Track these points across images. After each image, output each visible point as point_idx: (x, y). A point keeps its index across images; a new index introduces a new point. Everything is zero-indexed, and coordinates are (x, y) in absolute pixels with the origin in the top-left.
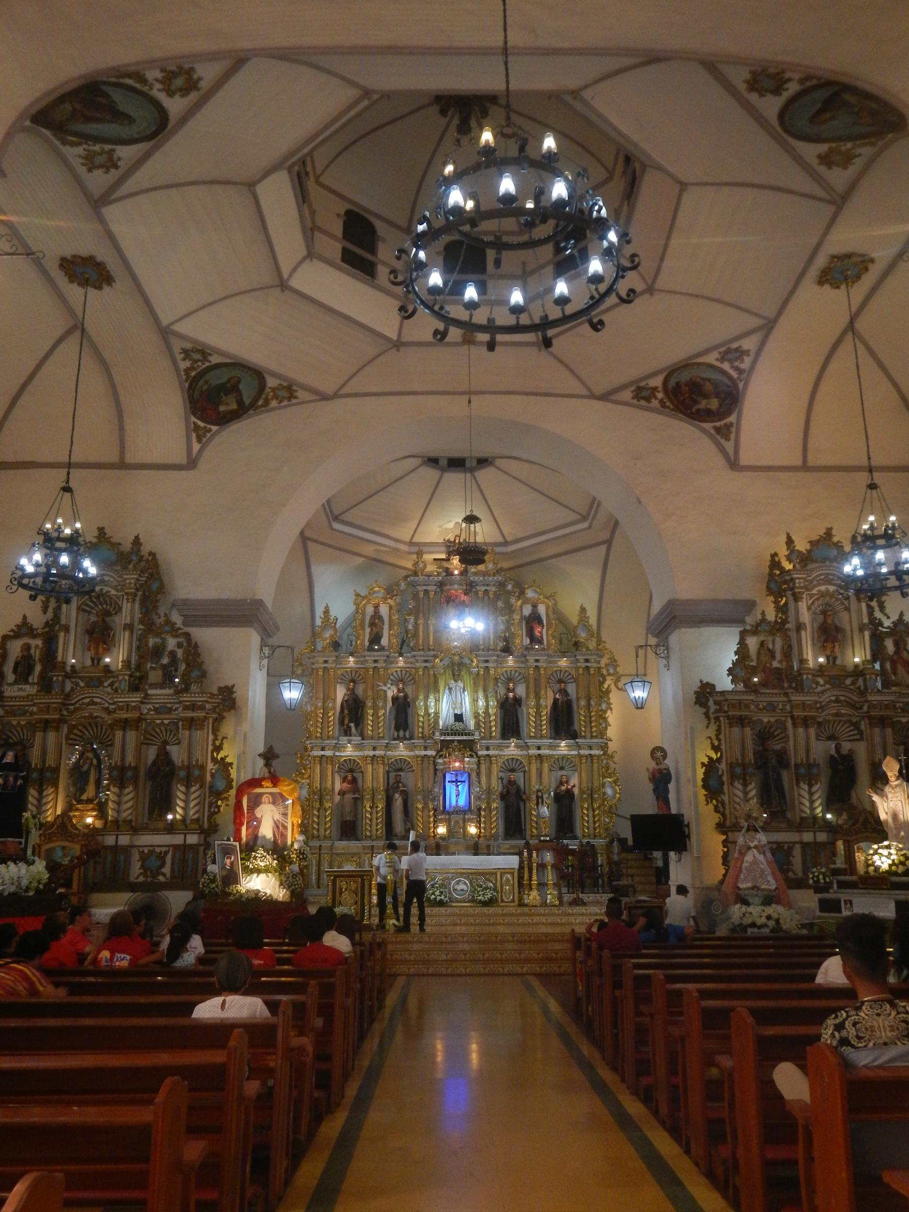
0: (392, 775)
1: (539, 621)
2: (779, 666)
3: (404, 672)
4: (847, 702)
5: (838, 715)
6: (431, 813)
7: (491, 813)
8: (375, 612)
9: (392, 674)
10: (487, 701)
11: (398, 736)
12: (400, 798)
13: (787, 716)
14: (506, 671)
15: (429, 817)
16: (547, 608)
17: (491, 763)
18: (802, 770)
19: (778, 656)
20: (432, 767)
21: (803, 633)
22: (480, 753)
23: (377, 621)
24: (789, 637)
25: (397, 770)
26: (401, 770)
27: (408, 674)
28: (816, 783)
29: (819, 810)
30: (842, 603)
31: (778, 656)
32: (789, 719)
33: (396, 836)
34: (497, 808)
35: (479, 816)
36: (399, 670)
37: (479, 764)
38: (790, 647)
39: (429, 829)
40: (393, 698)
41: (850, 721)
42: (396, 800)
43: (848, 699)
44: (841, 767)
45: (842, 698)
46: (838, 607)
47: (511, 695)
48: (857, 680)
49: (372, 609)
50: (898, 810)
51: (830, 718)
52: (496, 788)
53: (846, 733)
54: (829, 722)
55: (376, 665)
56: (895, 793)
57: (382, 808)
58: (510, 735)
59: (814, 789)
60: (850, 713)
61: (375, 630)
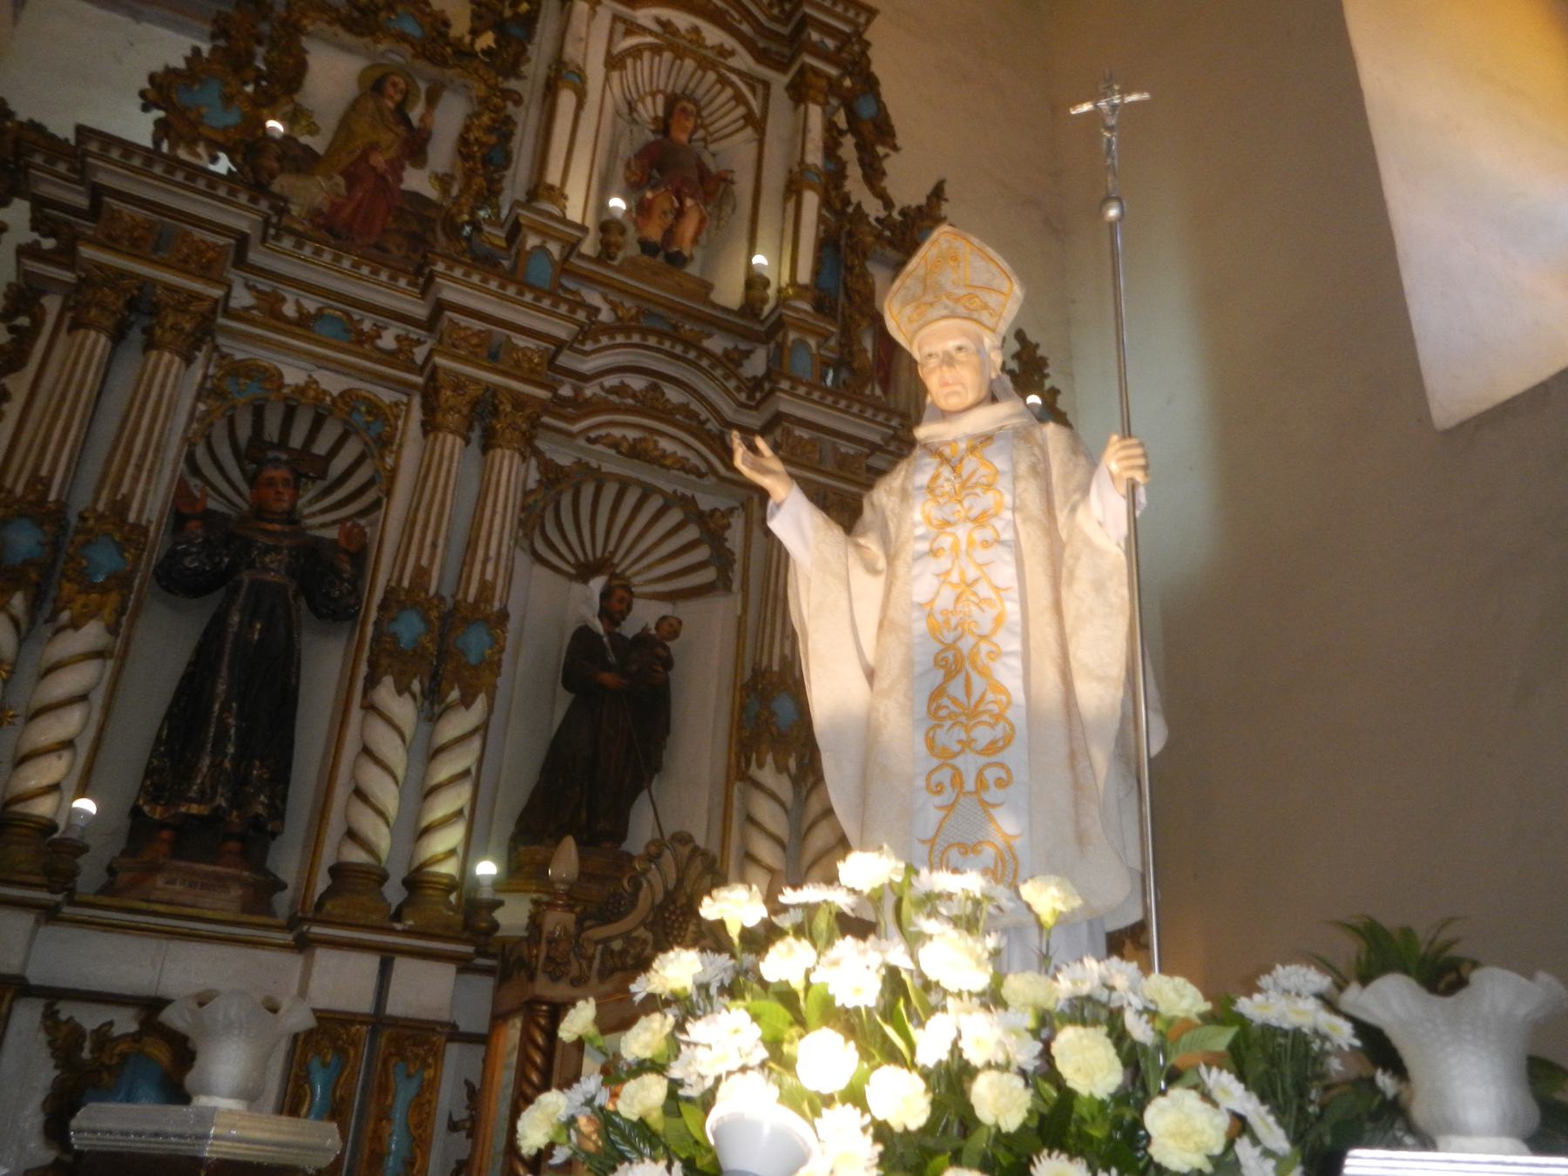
2: (431, 192)
4: (693, 415)
5: (635, 452)
13: (407, 387)
18: (409, 628)
19: (441, 153)
21: (566, 100)
24: (509, 121)
28: (466, 702)
29: (451, 838)
30: (739, 98)
31: (441, 153)
32: (417, 401)
38: (504, 129)
41: (687, 503)
43: (695, 406)
44: (608, 678)
45: (673, 395)
46: (723, 112)
48: (747, 354)
50: (984, 620)
51: (613, 465)
53: (663, 560)
54: (600, 480)
56: (966, 487)
59: (458, 723)
60: (695, 460)
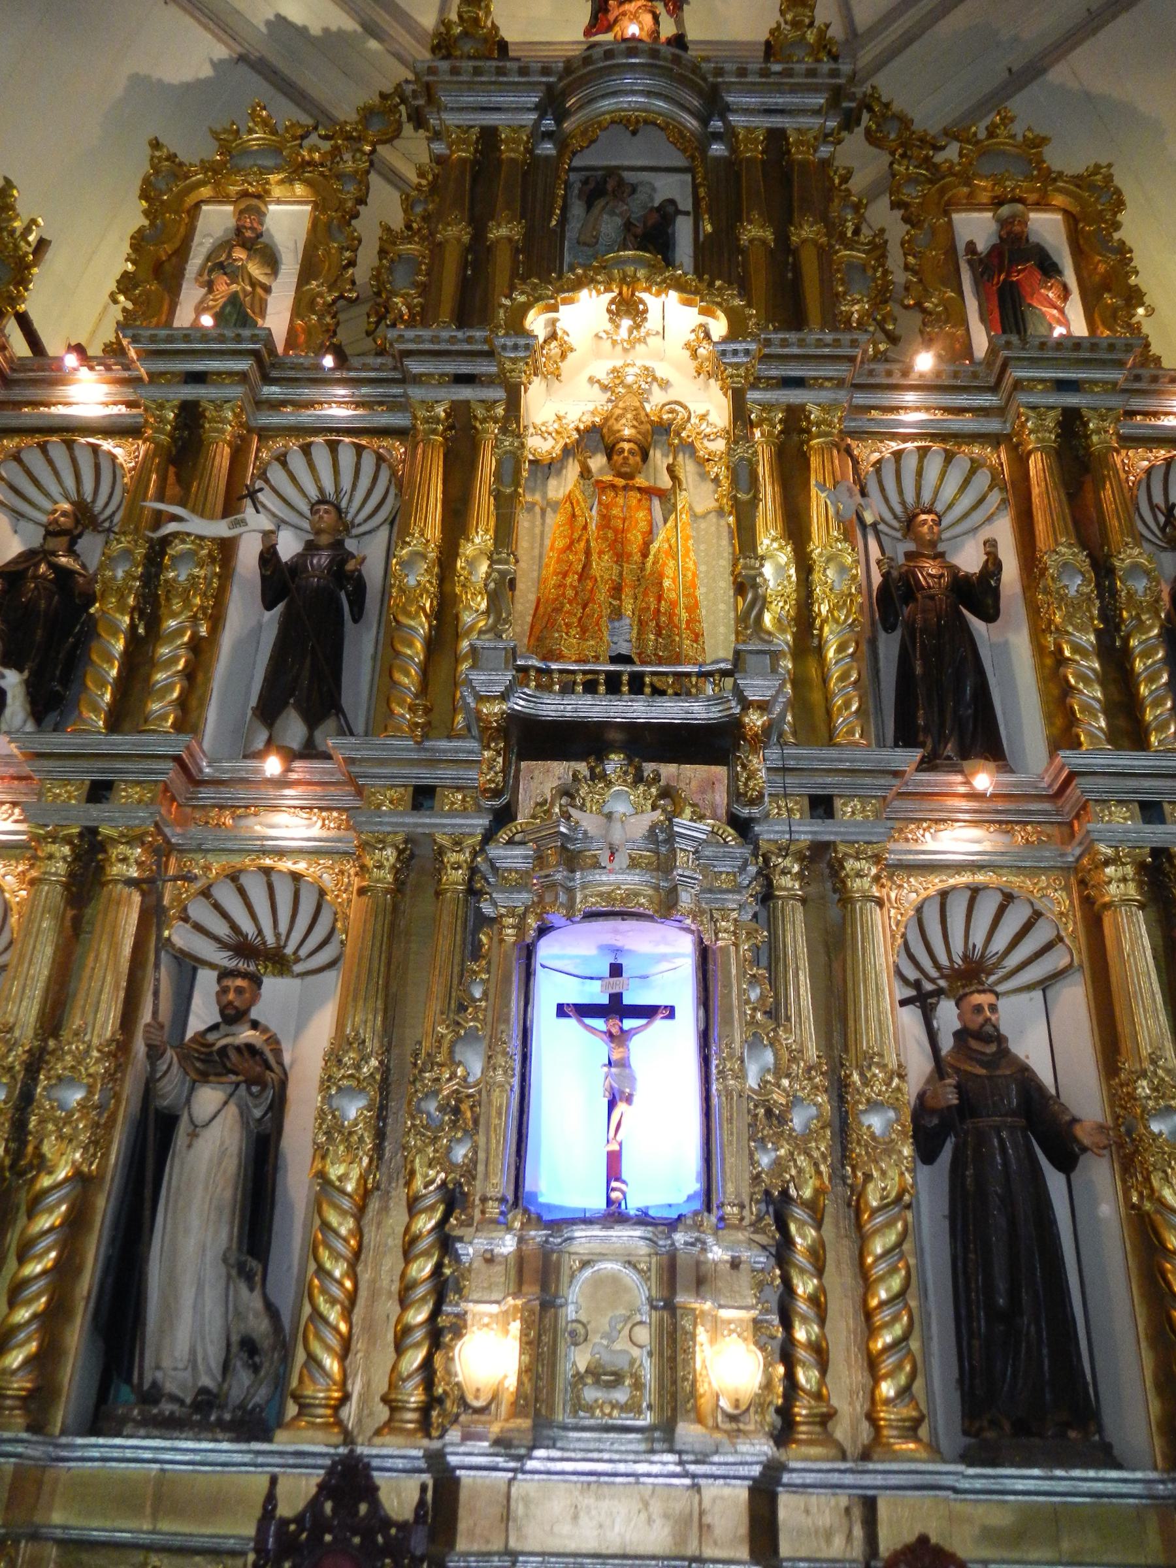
0: (206, 980)
1: (1049, 268)
3: (347, 457)
6: (425, 1223)
7: (862, 1240)
8: (239, 231)
9: (282, 459)
10: (804, 565)
11: (269, 742)
12: (232, 1110)
14: (898, 455)
15: (408, 1251)
16: (1072, 220)
17: (845, 899)
20: (449, 914)
22: (767, 833)
23: (239, 254)
25: (243, 948)
26: (279, 962)
27: (368, 461)
33: (152, 1395)
34: (899, 1202)
35: (783, 1251)
36: (319, 440)
37: (767, 896)
39: (400, 1349)
40: (268, 556)
42: (196, 1130)
47: (932, 568)
49: (231, 223)
52: (892, 1062)
55: (189, 392)
57: (81, 1180)
58: (950, 749)
61: (224, 288)
